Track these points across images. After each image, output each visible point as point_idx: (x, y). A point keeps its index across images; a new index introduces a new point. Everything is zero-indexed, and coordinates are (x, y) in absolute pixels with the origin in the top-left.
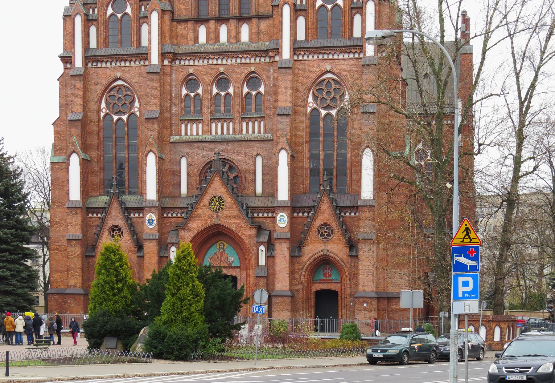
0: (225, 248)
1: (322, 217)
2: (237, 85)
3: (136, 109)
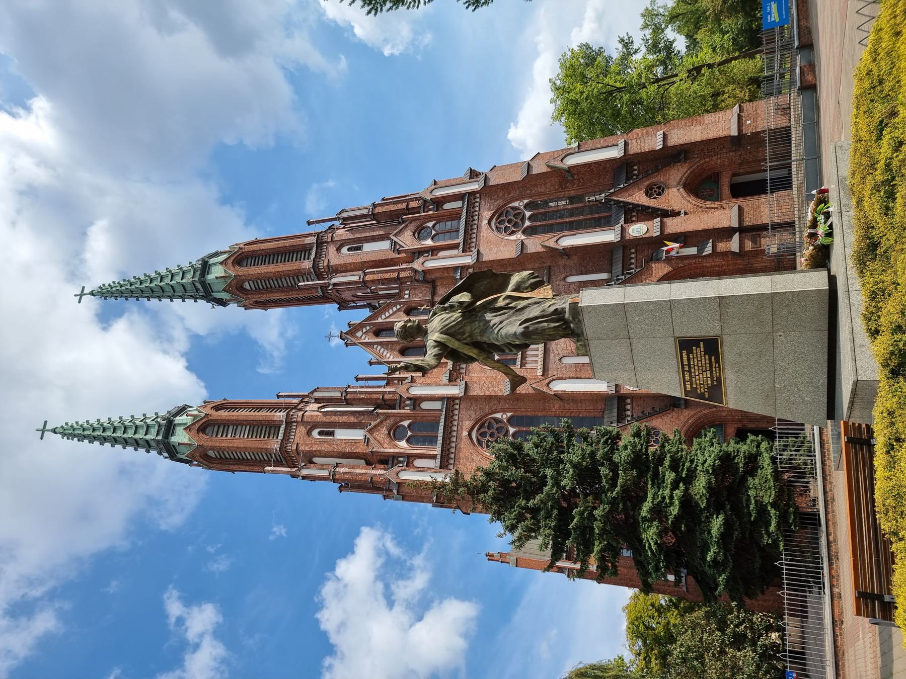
3: (504, 416)
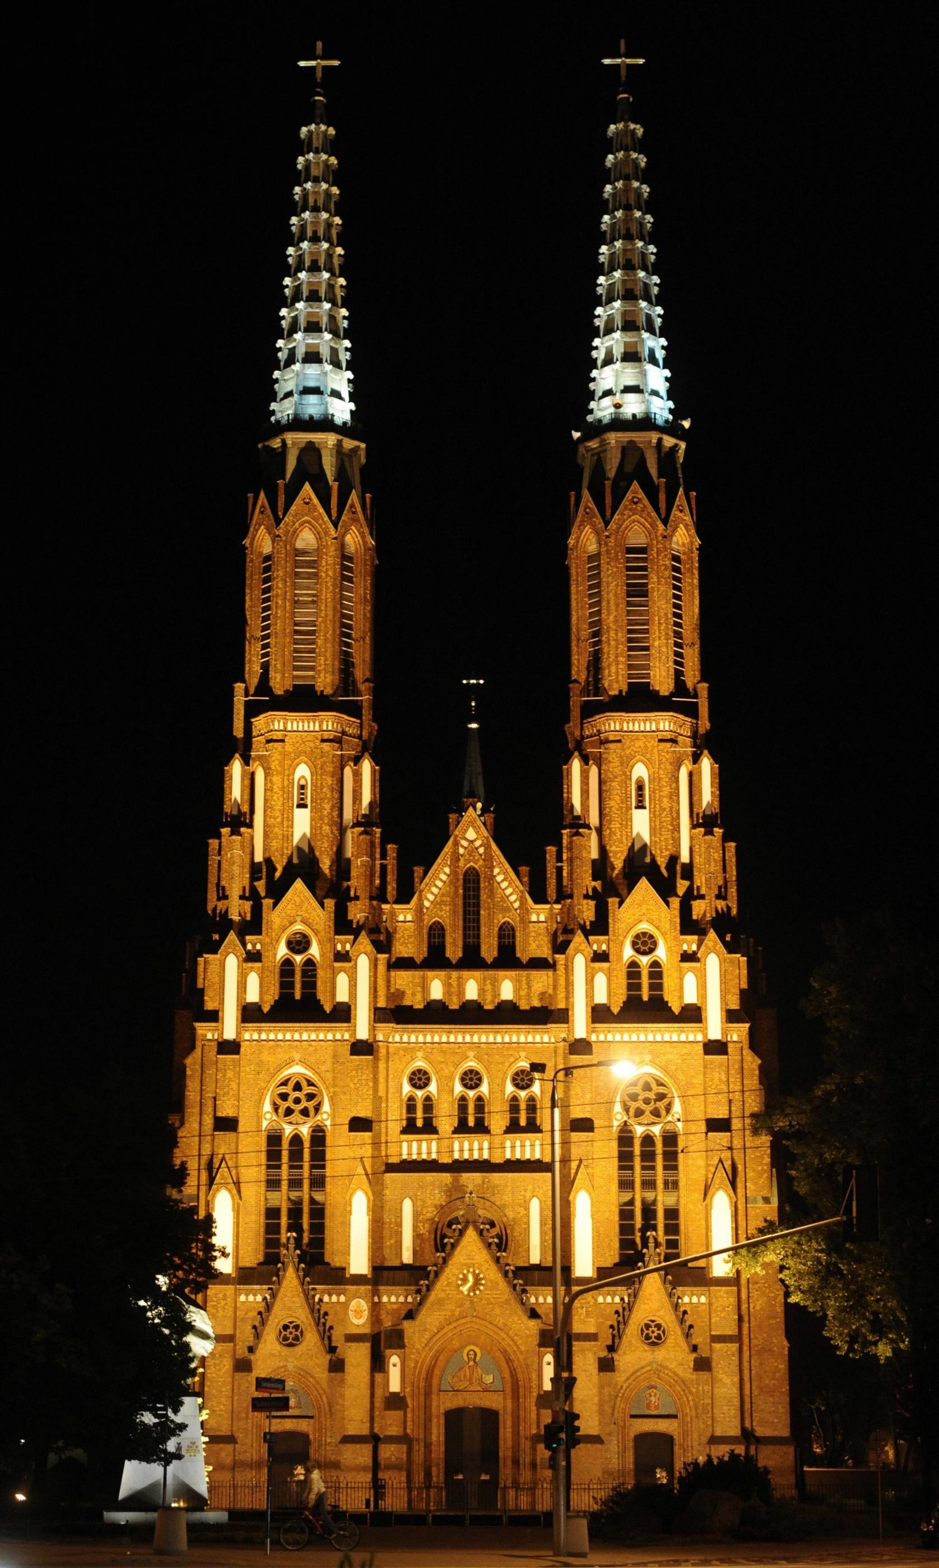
0: (478, 1358)
1: (646, 1306)
2: (497, 1081)
